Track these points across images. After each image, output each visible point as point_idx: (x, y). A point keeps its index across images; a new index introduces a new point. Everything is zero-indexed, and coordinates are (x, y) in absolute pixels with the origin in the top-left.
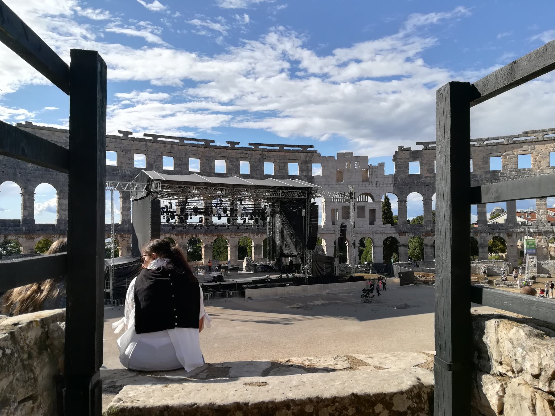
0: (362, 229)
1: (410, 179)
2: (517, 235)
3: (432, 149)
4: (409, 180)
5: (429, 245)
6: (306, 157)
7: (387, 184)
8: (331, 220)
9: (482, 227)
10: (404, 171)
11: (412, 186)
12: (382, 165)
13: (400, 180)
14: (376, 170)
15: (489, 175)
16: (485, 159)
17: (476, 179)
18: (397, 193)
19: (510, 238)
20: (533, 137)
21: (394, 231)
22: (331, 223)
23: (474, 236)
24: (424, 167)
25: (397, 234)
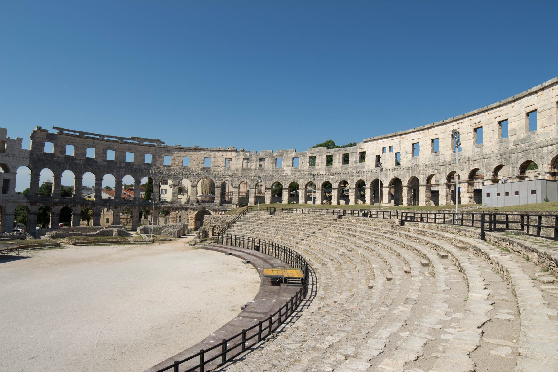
4: (44, 157)
7: (23, 158)
12: (20, 140)
13: (35, 156)
20: (136, 142)
21: (27, 201)
25: (29, 203)
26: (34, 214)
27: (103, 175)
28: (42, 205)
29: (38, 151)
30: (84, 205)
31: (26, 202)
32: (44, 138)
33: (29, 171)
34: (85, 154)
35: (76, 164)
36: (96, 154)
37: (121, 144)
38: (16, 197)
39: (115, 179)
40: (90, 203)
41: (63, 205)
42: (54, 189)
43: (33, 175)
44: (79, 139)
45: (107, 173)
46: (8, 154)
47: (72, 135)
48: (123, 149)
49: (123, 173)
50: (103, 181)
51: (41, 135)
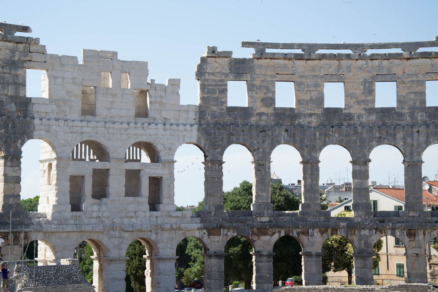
0: (134, 220)
1: (229, 116)
2: (424, 234)
3: (271, 59)
4: (228, 119)
5: (265, 253)
6: (13, 52)
8: (68, 200)
9: (363, 216)
10: (217, 99)
11: (234, 132)
13: (209, 117)
14: (163, 94)
15: (375, 117)
16: (367, 84)
17: (352, 122)
18: (205, 145)
19: (412, 239)
21: (199, 225)
22: (69, 207)
23: (347, 235)
24: (256, 93)
25: (205, 231)
26: (217, 256)
27: (370, 149)
28: (232, 234)
29: (214, 105)
30: (329, 231)
31: (198, 229)
32: (223, 72)
33: (200, 155)
34: (320, 100)
35: (302, 126)
36: (346, 96)
37: (411, 61)
38: (177, 217)
39: (401, 158)
40: (342, 224)
41: (280, 232)
42: (257, 193)
43: (208, 162)
44: (302, 63)
45: (380, 142)
46: (155, 119)
47: (285, 57)
48: (417, 75)
49: (422, 138)
50: (370, 164)
51: (217, 65)
